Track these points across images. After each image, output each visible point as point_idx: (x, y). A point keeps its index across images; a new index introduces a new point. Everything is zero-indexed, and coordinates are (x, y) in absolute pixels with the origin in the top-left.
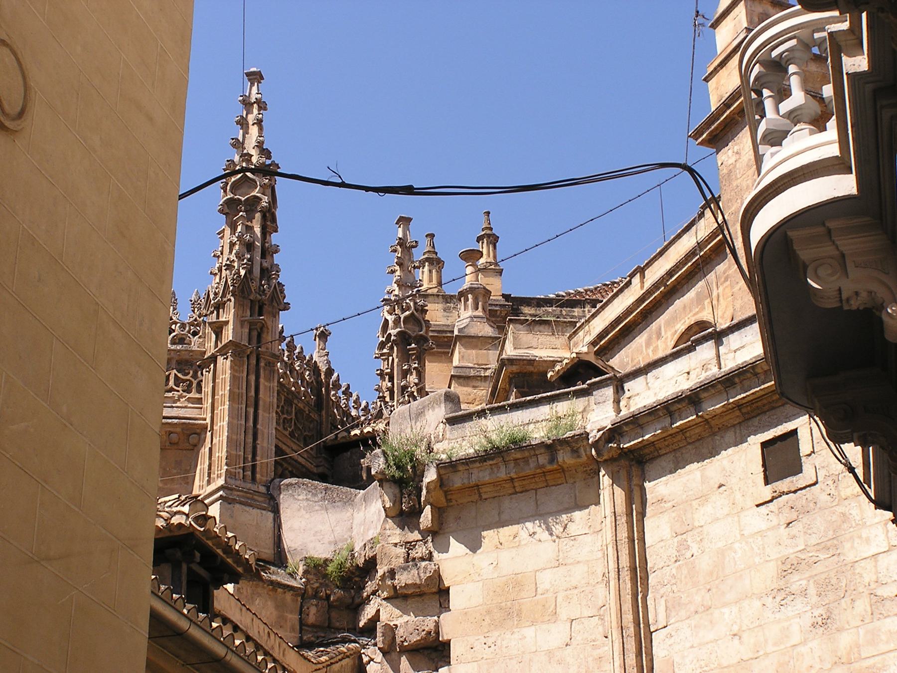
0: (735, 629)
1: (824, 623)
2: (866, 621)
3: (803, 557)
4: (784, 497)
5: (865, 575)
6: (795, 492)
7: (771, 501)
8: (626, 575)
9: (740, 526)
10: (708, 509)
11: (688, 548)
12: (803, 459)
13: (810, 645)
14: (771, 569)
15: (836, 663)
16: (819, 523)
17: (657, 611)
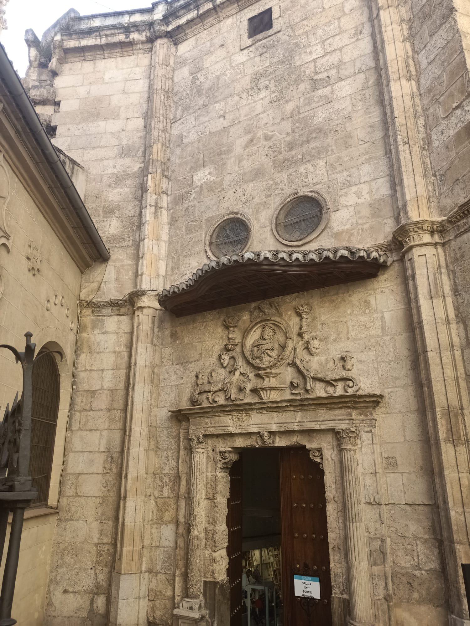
0: (222, 112)
4: (260, 43)
5: (307, 71)
6: (266, 38)
7: (251, 46)
10: (213, 58)
13: (267, 112)
14: (248, 79)
16: (279, 52)
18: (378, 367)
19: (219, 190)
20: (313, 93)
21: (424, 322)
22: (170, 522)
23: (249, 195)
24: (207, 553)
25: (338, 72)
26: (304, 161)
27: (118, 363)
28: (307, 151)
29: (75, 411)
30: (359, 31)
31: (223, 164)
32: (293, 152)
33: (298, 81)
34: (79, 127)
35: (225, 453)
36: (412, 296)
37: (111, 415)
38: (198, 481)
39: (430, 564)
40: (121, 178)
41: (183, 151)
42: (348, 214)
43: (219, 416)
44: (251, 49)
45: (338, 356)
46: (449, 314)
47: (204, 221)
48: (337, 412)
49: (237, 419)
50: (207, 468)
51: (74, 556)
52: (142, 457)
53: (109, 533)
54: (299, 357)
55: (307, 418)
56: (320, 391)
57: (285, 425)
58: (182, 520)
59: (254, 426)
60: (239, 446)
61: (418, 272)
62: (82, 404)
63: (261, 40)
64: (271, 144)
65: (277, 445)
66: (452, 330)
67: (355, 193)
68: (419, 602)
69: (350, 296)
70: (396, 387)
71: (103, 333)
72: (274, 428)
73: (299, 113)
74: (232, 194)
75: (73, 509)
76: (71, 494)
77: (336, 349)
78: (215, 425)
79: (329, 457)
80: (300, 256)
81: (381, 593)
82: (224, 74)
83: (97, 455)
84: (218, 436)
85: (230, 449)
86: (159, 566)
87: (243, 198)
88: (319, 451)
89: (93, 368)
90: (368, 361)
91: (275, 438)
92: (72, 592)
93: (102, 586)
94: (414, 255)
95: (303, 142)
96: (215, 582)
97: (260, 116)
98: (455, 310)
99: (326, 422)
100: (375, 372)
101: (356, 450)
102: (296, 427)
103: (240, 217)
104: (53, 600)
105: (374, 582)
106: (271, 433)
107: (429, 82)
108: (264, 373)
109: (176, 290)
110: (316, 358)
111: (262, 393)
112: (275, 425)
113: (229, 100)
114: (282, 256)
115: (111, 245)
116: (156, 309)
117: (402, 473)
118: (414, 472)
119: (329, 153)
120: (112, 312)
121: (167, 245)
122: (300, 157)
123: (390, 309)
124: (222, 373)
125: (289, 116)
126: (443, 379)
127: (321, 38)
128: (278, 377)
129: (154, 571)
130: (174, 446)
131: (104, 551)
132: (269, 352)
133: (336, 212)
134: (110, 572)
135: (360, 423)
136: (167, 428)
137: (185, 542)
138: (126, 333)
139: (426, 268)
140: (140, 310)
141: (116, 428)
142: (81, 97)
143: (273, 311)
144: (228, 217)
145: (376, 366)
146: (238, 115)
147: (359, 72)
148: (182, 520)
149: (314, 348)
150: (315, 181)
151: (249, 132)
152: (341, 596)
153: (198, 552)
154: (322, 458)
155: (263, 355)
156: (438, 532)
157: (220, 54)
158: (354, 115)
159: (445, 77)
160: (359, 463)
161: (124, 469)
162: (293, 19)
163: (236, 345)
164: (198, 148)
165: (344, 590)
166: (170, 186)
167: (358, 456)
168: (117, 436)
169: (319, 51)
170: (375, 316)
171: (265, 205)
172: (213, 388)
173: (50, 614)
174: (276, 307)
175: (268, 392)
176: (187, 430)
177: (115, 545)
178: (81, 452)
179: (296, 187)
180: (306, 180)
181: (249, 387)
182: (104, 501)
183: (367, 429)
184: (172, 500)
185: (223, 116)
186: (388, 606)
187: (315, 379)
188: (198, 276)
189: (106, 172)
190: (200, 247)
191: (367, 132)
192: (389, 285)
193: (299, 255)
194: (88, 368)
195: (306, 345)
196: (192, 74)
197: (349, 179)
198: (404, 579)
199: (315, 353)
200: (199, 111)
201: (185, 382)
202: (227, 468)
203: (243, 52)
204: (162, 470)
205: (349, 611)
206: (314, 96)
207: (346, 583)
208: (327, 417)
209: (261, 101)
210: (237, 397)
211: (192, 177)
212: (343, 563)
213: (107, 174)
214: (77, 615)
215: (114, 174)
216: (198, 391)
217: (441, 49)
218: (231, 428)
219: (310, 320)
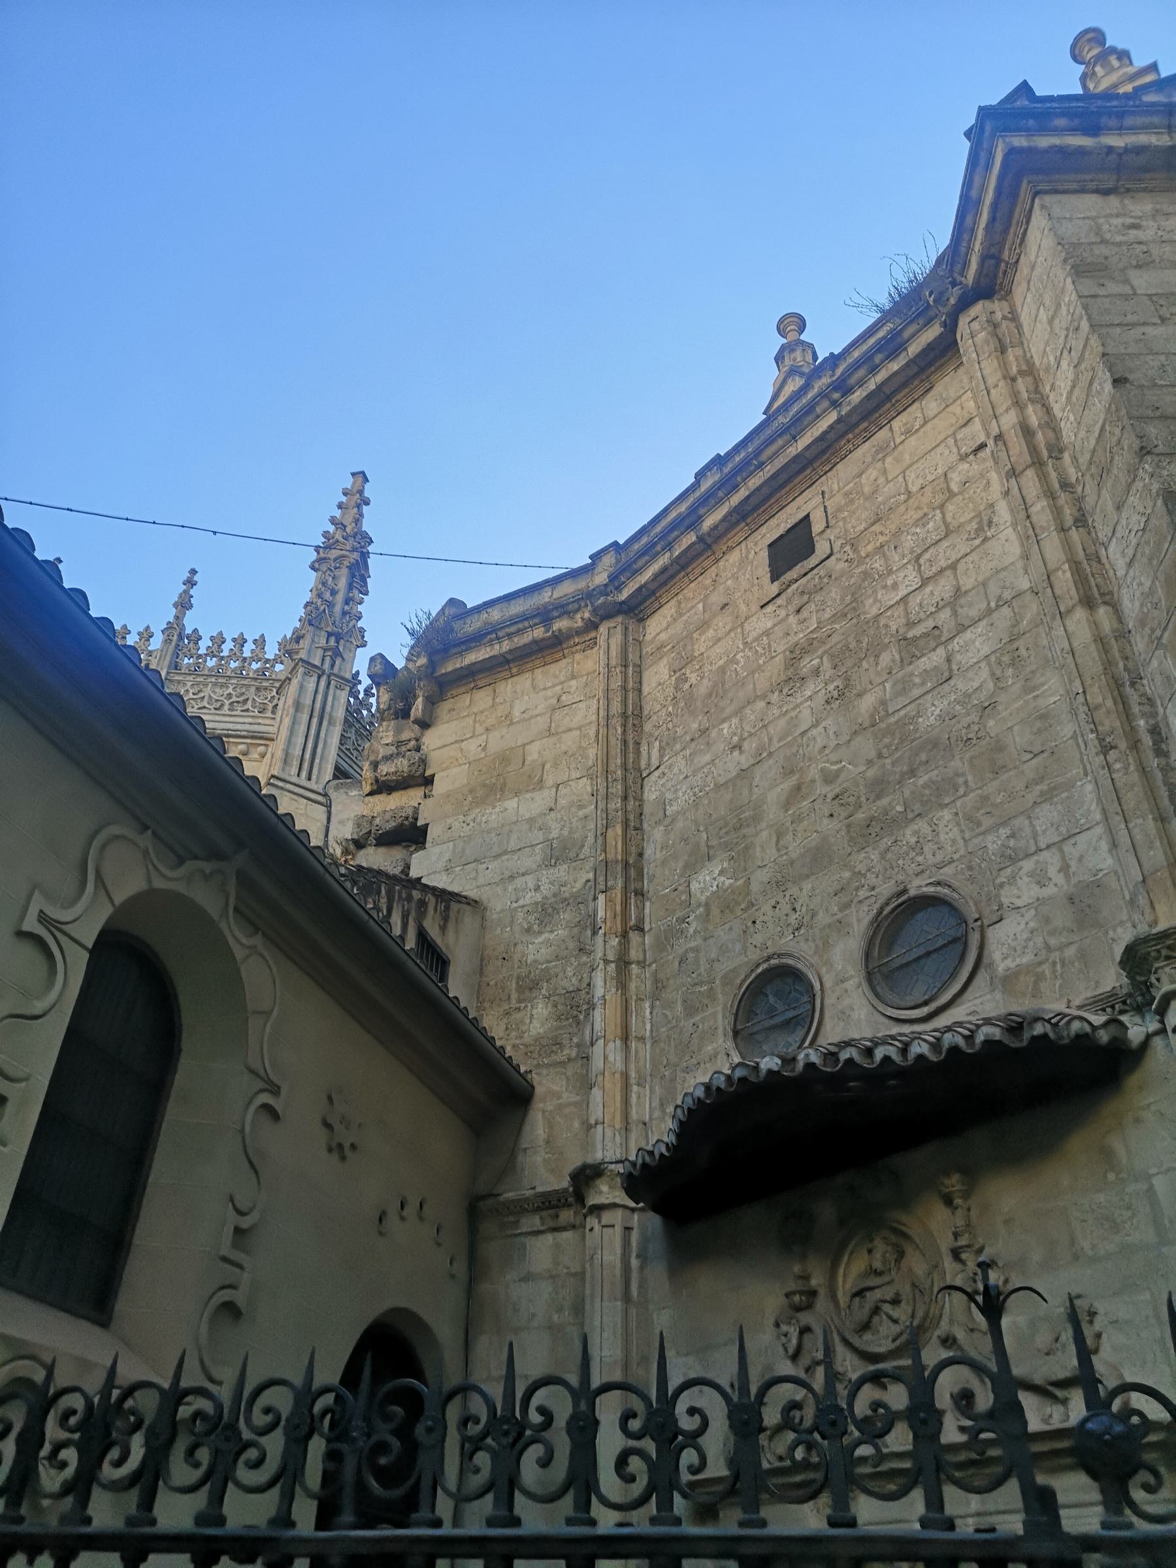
1: (842, 696)
2: (894, 672)
3: (815, 636)
4: (794, 586)
6: (805, 574)
7: (778, 595)
8: (617, 723)
9: (743, 634)
10: (710, 633)
11: (686, 680)
12: (815, 539)
13: (824, 724)
15: (856, 731)
17: (651, 753)
19: (743, 906)
20: (911, 667)
23: (804, 909)
25: (955, 613)
26: (910, 816)
28: (913, 793)
30: (985, 522)
31: (747, 848)
32: (885, 801)
33: (875, 650)
34: (469, 819)
40: (550, 910)
41: (667, 832)
42: (1023, 926)
44: (779, 601)
47: (718, 982)
63: (797, 580)
64: (837, 790)
67: (1031, 874)
73: (888, 715)
74: (770, 912)
82: (733, 661)
87: (793, 919)
95: (903, 774)
97: (809, 734)
103: (790, 962)
107: (1137, 604)
109: (647, 1159)
113: (748, 711)
115: (535, 1062)
116: (633, 1210)
119: (961, 791)
122: (899, 808)
123: (1165, 1167)
125: (866, 724)
127: (912, 552)
132: (887, 1308)
133: (996, 926)
142: (471, 759)
144: (765, 966)
146: (766, 739)
147: (998, 607)
150: (939, 857)
151: (792, 772)
157: (722, 622)
158: (1002, 698)
159: (1160, 590)
162: (854, 527)
164: (696, 822)
166: (647, 911)
169: (910, 578)
170: (1131, 1188)
171: (840, 926)
179: (900, 877)
180: (920, 859)
185: (738, 747)
189: (521, 902)
191: (1035, 730)
196: (675, 672)
197: (1012, 843)
200: (693, 745)
203: (764, 611)
206: (912, 674)
209: (809, 703)
211: (689, 886)
213: (523, 907)
215: (537, 903)
217: (1140, 533)
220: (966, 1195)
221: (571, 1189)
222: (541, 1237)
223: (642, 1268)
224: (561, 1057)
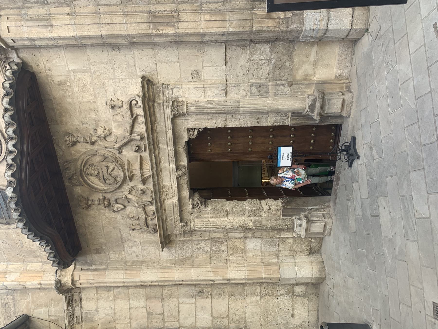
18: (119, 79)
21: (74, 34)
22: (244, 243)
24: (264, 215)
27: (124, 296)
29: (164, 327)
35: (194, 204)
36: (51, 43)
37: (167, 297)
38: (215, 224)
39: (267, 51)
43: (165, 210)
45: (111, 112)
46: (66, 12)
48: (158, 115)
49: (167, 196)
50: (205, 218)
51: (269, 313)
52: (198, 270)
53: (253, 288)
54: (113, 144)
55: (164, 140)
56: (141, 128)
57: (170, 157)
58: (242, 235)
59: (172, 182)
60: (188, 193)
61: (26, 35)
62: (158, 322)
65: (186, 164)
66: (82, 11)
68: (292, 62)
69: (54, 98)
70: (135, 65)
71: (97, 311)
72: (173, 166)
75: (237, 318)
76: (227, 321)
77: (105, 113)
78: (173, 214)
79: (193, 123)
80: (11, 143)
81: (286, 89)
83: (198, 304)
84: (181, 210)
85: (191, 200)
86: (274, 250)
88: (189, 131)
89: (129, 317)
90: (114, 86)
91: (182, 165)
92: (293, 311)
93: (288, 290)
94: (8, 36)
96: (283, 209)
98: (62, 6)
99: (167, 125)
100: (123, 81)
101: (187, 102)
102: (172, 149)
104: (298, 324)
105: (279, 94)
106: (177, 169)
108: (129, 174)
110: (114, 130)
111: (145, 176)
112: (171, 166)
114: (11, 160)
115: (12, 315)
116: (75, 268)
117: (203, 67)
118: (202, 57)
120: (78, 306)
121: (11, 263)
123: (66, 64)
124: (130, 209)
126: (125, 25)
128: (131, 162)
129: (277, 253)
130: (189, 244)
131: (266, 291)
134: (279, 285)
135: (166, 97)
136: (176, 251)
137: (257, 232)
138: (97, 292)
139: (22, 28)
140: (75, 283)
141: (177, 292)
143: (72, 166)
145: (118, 80)
148: (242, 235)
149: (104, 132)
152: (290, 119)
153: (264, 222)
154: (195, 129)
155: (113, 175)
156: (245, 43)
160: (197, 100)
161: (207, 282)
163: (105, 198)
165: (285, 116)
167: (191, 101)
168: (183, 290)
170: (73, 78)
172: (143, 216)
173: (307, 325)
174: (68, 164)
175: (144, 170)
176: (176, 236)
177: (261, 283)
178: (196, 318)
181: (141, 186)
182: (232, 295)
183: (170, 92)
184: (229, 243)
186: (295, 84)
187: (131, 133)
188: (35, 238)
190: (12, 233)
192: (42, 63)
193: (9, 144)
194: (128, 321)
195: (102, 138)
198: (277, 71)
199: (109, 131)
201: (139, 240)
202: (205, 202)
204: (207, 252)
205: (299, 113)
207: (281, 114)
208: (162, 124)
210: (150, 195)
212: (268, 116)
214: (307, 305)
216: (146, 228)
218: (174, 201)
219: (79, 135)
220: (73, 136)
221: (66, 294)
222: (83, 306)
223: (95, 265)
224: (11, 302)
